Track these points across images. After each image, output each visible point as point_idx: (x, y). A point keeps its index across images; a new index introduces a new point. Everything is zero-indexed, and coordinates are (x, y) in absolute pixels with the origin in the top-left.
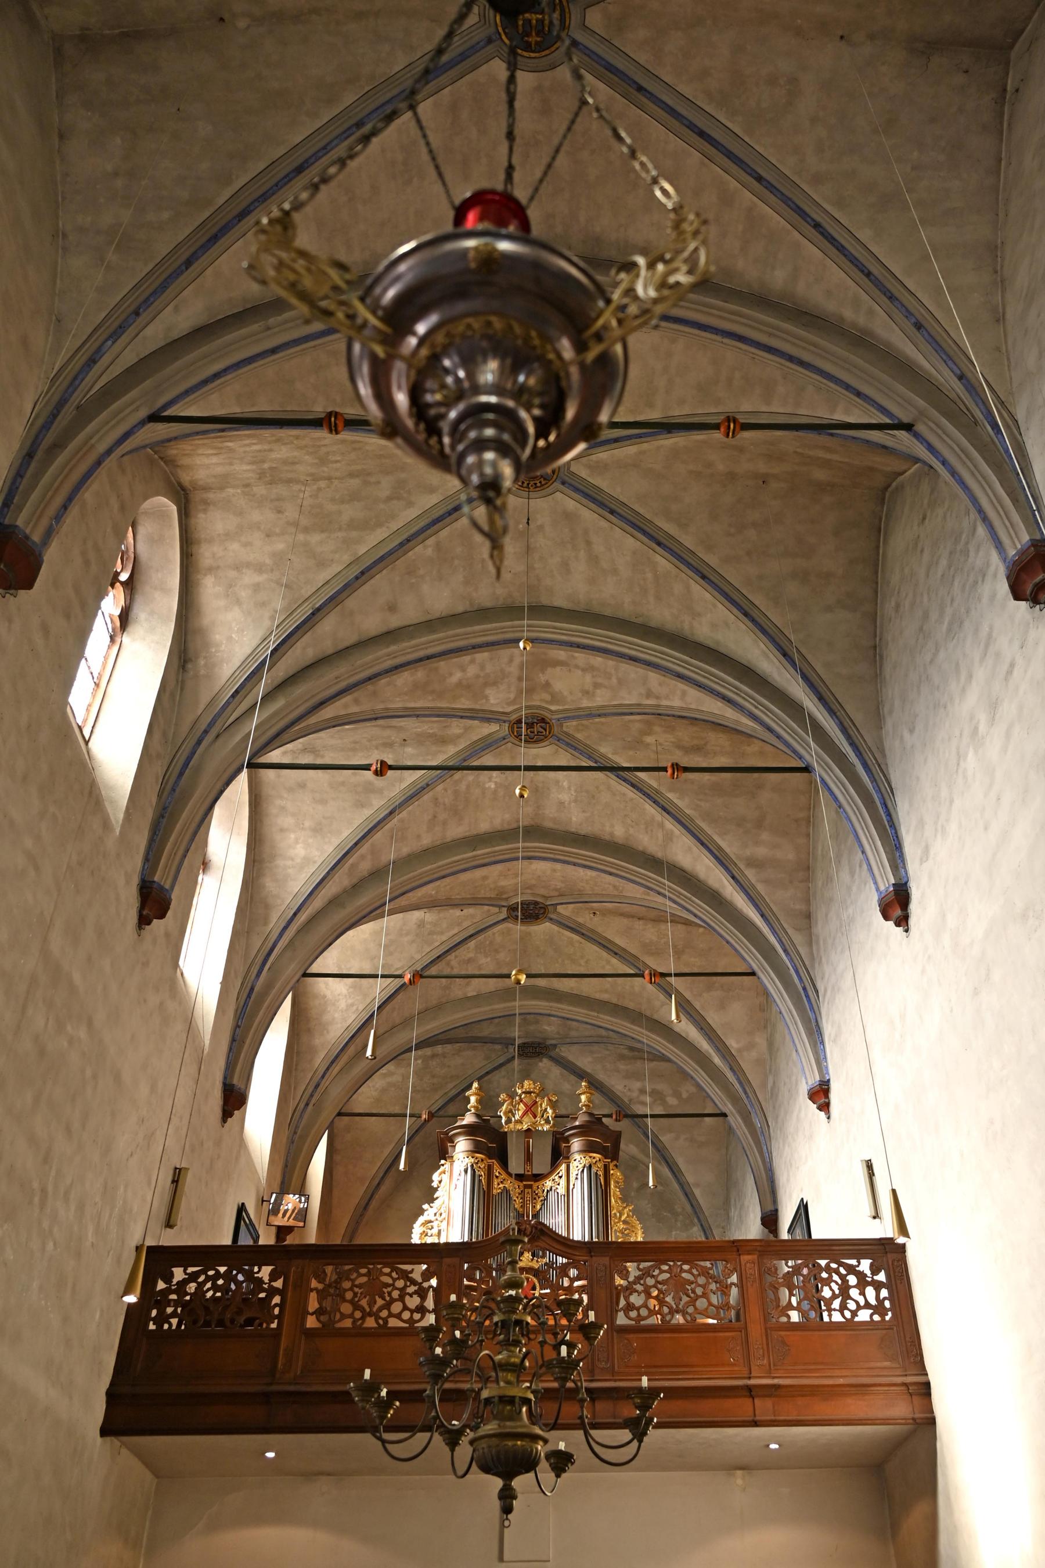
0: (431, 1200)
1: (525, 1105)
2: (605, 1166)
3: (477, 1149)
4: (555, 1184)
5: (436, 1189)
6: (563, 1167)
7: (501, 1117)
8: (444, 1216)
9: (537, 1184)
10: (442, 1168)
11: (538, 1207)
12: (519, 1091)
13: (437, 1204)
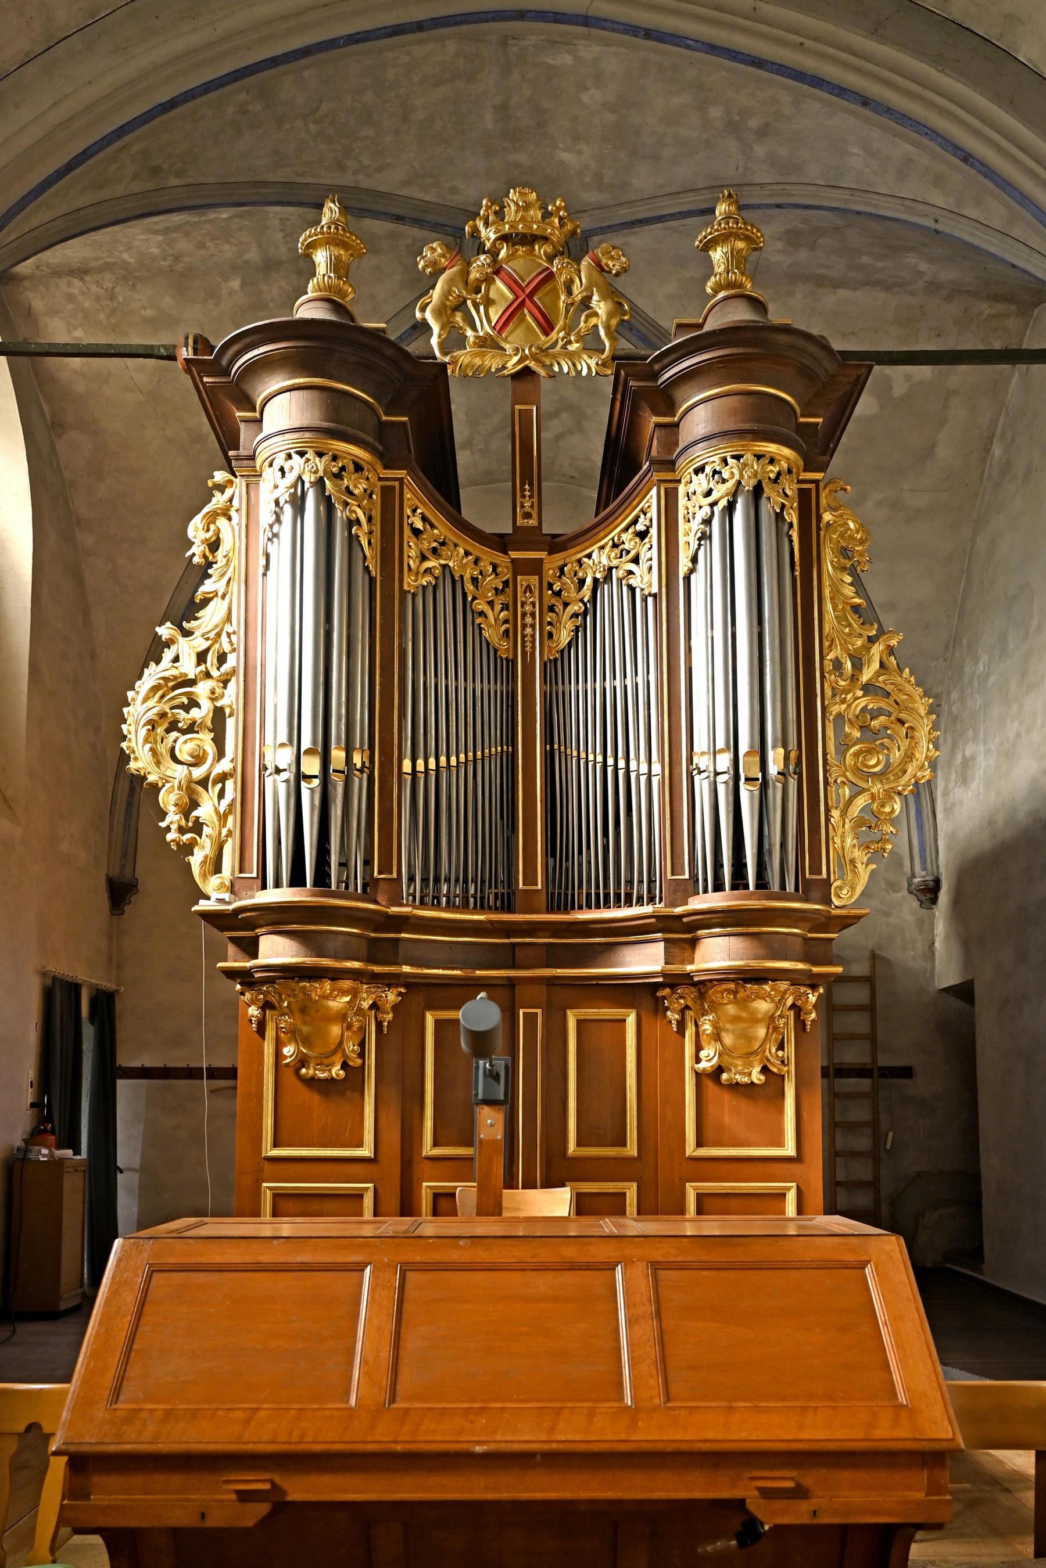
0: (186, 611)
1: (513, 284)
3: (336, 423)
4: (624, 560)
6: (652, 499)
7: (423, 328)
8: (231, 661)
9: (558, 559)
10: (219, 500)
11: (564, 637)
12: (489, 235)
13: (210, 617)
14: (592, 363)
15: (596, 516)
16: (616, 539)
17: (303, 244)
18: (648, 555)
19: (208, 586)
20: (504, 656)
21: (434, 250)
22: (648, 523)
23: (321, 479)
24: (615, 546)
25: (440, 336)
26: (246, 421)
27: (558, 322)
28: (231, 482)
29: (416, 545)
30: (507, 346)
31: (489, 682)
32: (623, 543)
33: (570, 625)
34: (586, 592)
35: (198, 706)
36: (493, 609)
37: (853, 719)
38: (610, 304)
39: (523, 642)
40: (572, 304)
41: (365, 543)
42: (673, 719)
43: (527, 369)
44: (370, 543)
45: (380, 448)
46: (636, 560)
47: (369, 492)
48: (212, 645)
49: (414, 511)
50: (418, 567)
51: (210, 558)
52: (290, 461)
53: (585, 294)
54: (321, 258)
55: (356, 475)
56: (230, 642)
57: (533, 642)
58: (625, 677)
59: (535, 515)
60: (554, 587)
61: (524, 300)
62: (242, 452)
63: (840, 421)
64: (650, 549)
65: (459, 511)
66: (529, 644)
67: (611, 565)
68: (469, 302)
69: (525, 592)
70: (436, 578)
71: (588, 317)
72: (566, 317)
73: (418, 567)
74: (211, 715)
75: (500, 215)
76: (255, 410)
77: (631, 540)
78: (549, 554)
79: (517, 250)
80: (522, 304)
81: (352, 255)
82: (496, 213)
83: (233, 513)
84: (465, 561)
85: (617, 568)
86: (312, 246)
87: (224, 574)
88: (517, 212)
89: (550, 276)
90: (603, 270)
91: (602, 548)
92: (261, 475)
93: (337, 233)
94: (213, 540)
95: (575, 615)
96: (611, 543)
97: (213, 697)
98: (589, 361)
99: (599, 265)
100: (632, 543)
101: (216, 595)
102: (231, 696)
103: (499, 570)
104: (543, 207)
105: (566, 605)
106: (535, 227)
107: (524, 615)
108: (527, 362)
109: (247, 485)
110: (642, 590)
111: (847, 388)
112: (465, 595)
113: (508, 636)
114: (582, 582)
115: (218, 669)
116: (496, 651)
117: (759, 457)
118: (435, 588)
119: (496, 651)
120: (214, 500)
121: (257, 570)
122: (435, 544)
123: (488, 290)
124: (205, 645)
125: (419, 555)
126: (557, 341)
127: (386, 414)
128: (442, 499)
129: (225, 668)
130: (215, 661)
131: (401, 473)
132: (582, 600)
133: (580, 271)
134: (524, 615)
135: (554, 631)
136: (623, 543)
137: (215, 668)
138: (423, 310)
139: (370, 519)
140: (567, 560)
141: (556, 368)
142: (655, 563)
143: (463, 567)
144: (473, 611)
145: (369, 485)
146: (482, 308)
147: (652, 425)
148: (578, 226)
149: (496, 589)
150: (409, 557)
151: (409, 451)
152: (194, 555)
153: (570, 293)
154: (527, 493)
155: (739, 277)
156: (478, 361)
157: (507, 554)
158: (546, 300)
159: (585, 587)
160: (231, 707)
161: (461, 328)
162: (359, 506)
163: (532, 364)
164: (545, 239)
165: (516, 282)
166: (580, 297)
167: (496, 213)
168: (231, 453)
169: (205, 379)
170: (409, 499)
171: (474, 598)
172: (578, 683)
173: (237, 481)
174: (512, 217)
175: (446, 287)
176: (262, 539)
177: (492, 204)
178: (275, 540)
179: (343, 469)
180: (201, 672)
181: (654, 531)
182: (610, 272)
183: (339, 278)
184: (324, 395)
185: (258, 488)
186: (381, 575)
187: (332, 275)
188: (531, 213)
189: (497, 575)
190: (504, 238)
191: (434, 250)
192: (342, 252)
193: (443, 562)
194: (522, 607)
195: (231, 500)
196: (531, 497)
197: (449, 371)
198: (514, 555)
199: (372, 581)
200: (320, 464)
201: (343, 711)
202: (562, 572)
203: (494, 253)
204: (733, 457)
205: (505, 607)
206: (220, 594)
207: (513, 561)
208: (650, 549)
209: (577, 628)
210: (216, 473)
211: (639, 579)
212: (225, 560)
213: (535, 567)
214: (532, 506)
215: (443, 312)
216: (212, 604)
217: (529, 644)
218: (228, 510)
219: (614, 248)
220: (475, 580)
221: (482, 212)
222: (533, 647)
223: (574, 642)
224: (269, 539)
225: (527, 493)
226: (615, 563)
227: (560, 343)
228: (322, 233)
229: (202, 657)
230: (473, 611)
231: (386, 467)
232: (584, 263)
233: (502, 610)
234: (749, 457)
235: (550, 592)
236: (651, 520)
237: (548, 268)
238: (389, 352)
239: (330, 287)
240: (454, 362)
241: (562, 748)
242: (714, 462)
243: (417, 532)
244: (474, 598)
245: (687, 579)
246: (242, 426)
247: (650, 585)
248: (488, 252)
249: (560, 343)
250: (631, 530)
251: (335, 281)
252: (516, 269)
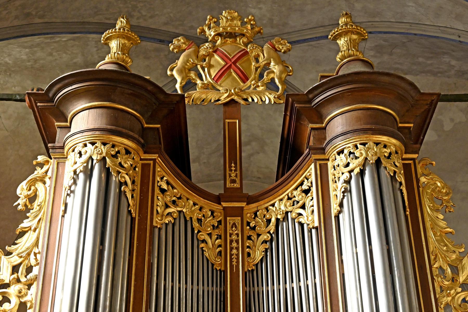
1: (224, 57)
2: (406, 167)
5: (23, 215)
8: (35, 271)
9: (253, 206)
10: (39, 172)
11: (258, 255)
12: (210, 33)
13: (25, 242)
14: (272, 97)
15: (276, 181)
16: (290, 194)
17: (104, 38)
18: (311, 203)
19: (26, 224)
20: (218, 268)
21: (179, 41)
22: (310, 184)
23: (104, 158)
24: (289, 199)
25: (181, 83)
26: (60, 127)
27: (251, 76)
28: (47, 162)
29: (163, 199)
30: (221, 89)
31: (208, 286)
32: (295, 197)
33: (262, 248)
34: (272, 227)
35: (9, 302)
36: (211, 238)
37: (457, 307)
38: (281, 67)
39: (231, 259)
40: (259, 67)
41: (129, 196)
42: (334, 308)
43: (233, 100)
44: (132, 196)
45: (142, 141)
46: (303, 207)
47: (134, 166)
48: (23, 261)
49: (162, 178)
50: (163, 212)
51: (29, 206)
52: (86, 148)
53: (266, 62)
54: (114, 44)
55: (126, 156)
56: (36, 259)
57: (238, 259)
58: (299, 281)
59: (238, 180)
60: (251, 224)
61: (231, 65)
62: (57, 144)
63: (423, 126)
64: (312, 200)
65: (190, 178)
66: (234, 260)
67: (287, 210)
68: (199, 67)
69: (232, 227)
70: (175, 219)
71: (268, 73)
72: (255, 74)
73: (163, 212)
74: (17, 307)
75: (217, 23)
76: (67, 122)
77: (299, 194)
78: (247, 204)
79: (227, 41)
80: (230, 67)
81: (132, 43)
82: (215, 22)
83: (47, 180)
84: (193, 209)
85: (291, 212)
86: (109, 39)
87: (37, 216)
88: (227, 22)
89: (247, 53)
90: (276, 50)
91: (281, 200)
92: (67, 158)
93: (124, 32)
94: (32, 195)
95: (265, 242)
96: (286, 197)
97: (20, 295)
98: (269, 96)
99: (274, 47)
100: (300, 197)
101: (30, 229)
102: (32, 295)
103: (215, 214)
104: (242, 20)
105: (259, 235)
106: (237, 29)
107: (231, 241)
108: (233, 97)
109: (58, 163)
110: (308, 225)
111: (427, 107)
112: (193, 230)
113: (221, 255)
114: (269, 221)
115: (26, 277)
116: (213, 265)
117: (377, 144)
118: (174, 225)
119: (213, 265)
120: (36, 172)
121: (59, 214)
122: (174, 198)
123: (210, 60)
124: (20, 260)
125: (164, 204)
126: (250, 87)
127: (147, 123)
128: (179, 171)
129: (31, 276)
130: (24, 271)
131: (155, 156)
132: (269, 232)
133: (263, 51)
134: (231, 241)
135: (251, 252)
136: (295, 197)
137: (23, 276)
138: (172, 70)
139: (133, 182)
140: (259, 208)
141: (250, 100)
142: (315, 208)
143: (192, 212)
144: (198, 240)
145: (134, 162)
146: (206, 69)
147: (309, 129)
148: (261, 29)
149: (213, 226)
150: (157, 205)
151: (160, 143)
152: (19, 204)
153: (257, 61)
154: (233, 168)
155: (355, 53)
156: (204, 96)
157: (220, 204)
158: (244, 65)
159: (271, 224)
160: (31, 302)
161: (194, 79)
162: (127, 174)
163: (236, 98)
164: (243, 35)
165: (226, 56)
166: (264, 63)
167: (215, 22)
168: (49, 145)
169: (38, 104)
170: (159, 171)
171: (199, 232)
172: (267, 285)
173: (52, 161)
174: (224, 24)
175: (186, 59)
176: (64, 194)
177: (213, 18)
178: (72, 195)
179: (118, 152)
180: (14, 278)
181: (314, 189)
182: (280, 51)
183: (123, 54)
184: (109, 111)
185: (65, 165)
186: (139, 216)
187: (120, 53)
188: (235, 22)
189: (214, 217)
190: (219, 35)
191: (179, 41)
192: (126, 42)
193: (179, 209)
194: (230, 236)
195: (46, 172)
196: (235, 171)
197: (186, 102)
198: (224, 204)
199: (133, 220)
200: (104, 149)
201: (108, 303)
202: (256, 215)
203: (214, 41)
204: (361, 144)
205: (219, 237)
206: (33, 228)
207: (224, 208)
208: (312, 200)
209: (266, 250)
210: (39, 157)
211: (306, 218)
212: (38, 208)
213: (239, 212)
214: (236, 176)
215: (183, 71)
216: (27, 235)
217: (234, 260)
218: (44, 178)
219: (282, 39)
220: (199, 220)
221: (207, 22)
222: (238, 262)
223: (265, 257)
224: (68, 195)
225: (233, 168)
226: (290, 209)
227: (252, 87)
228: (115, 32)
229: (15, 269)
230: (198, 240)
231: (145, 153)
232: (265, 47)
233: (217, 239)
234: (371, 144)
235: (248, 227)
236: (312, 183)
237: (244, 49)
238: (150, 88)
239: (118, 59)
240: (189, 97)
242: (349, 147)
243: (163, 191)
244: (199, 232)
245: (337, 217)
246: (58, 130)
247: (313, 222)
248: (210, 41)
249: (252, 87)
250: (299, 189)
251: (121, 56)
252: (227, 49)
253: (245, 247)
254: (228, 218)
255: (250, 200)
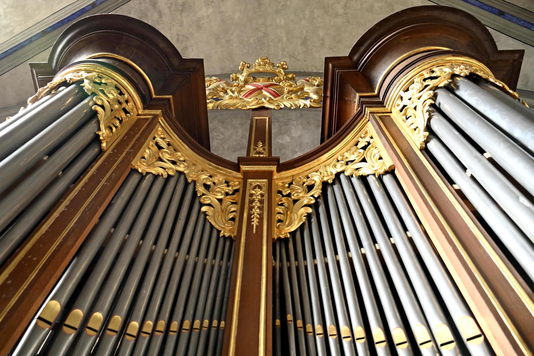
116: (219, 232)
241: (300, 323)
253: (274, 203)
254: (250, 180)
255: (283, 167)
